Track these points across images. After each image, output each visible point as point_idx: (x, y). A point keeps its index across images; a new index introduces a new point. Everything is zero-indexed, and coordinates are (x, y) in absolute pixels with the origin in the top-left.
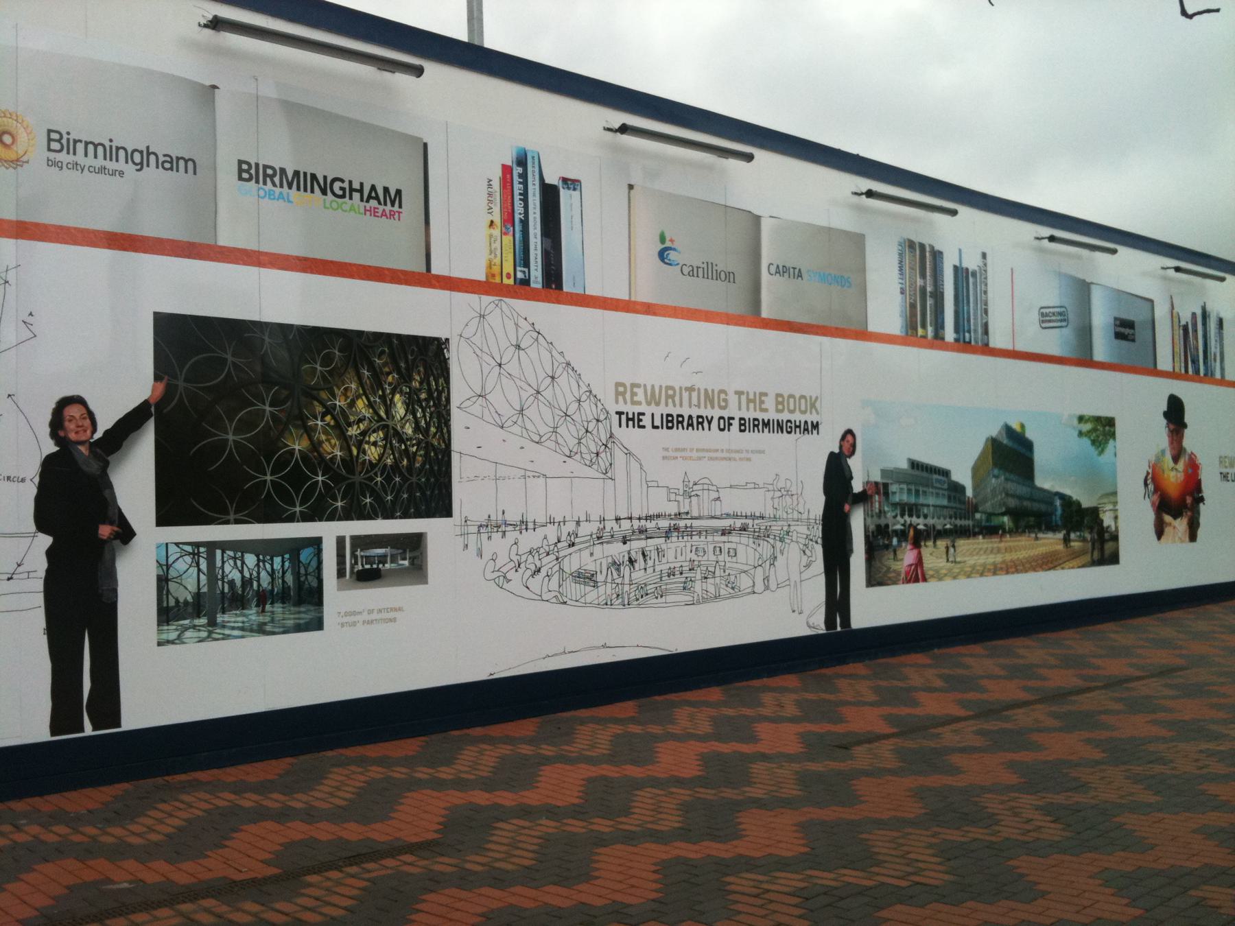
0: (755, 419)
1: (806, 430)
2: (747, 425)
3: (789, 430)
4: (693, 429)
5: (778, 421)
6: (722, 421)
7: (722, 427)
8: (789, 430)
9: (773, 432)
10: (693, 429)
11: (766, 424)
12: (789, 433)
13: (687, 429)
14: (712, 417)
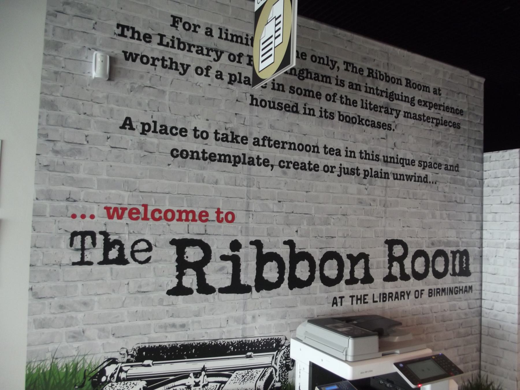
0: (438, 289)
1: (466, 291)
2: (433, 293)
3: (456, 292)
4: (398, 300)
5: (450, 288)
6: (417, 293)
7: (417, 296)
8: (456, 292)
9: (447, 295)
10: (398, 300)
11: (443, 290)
12: (456, 294)
13: (395, 300)
14: (410, 292)
